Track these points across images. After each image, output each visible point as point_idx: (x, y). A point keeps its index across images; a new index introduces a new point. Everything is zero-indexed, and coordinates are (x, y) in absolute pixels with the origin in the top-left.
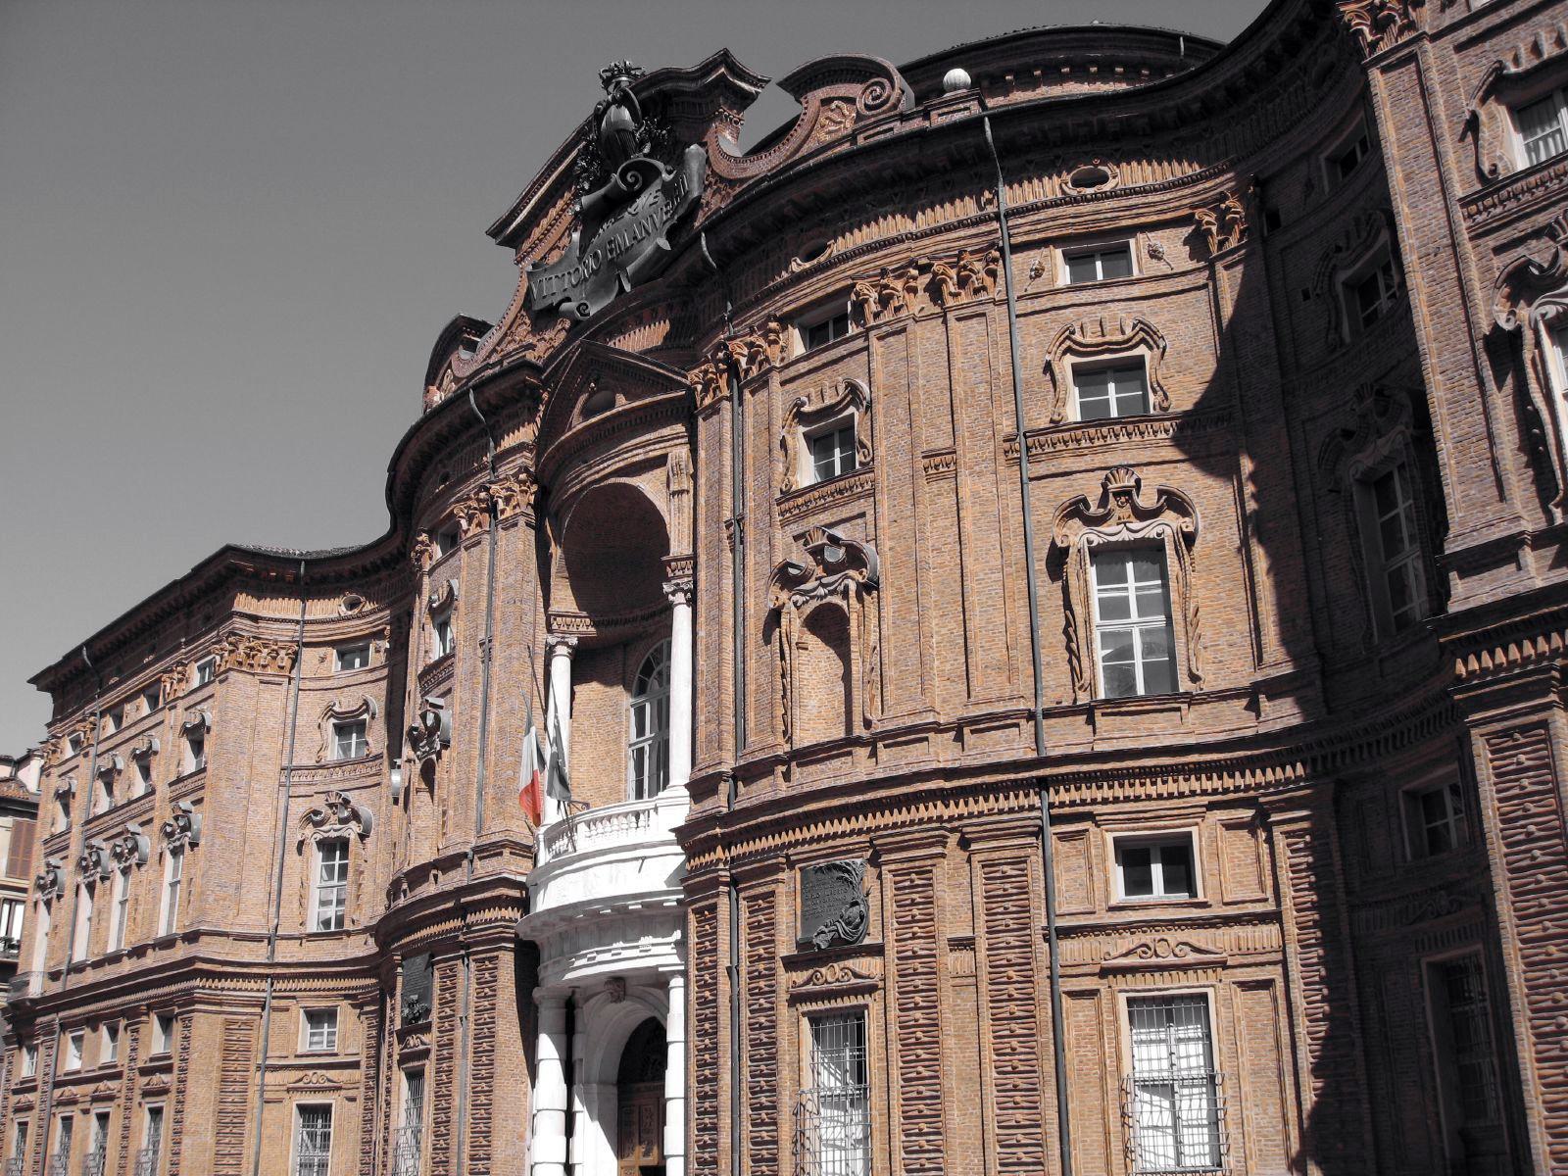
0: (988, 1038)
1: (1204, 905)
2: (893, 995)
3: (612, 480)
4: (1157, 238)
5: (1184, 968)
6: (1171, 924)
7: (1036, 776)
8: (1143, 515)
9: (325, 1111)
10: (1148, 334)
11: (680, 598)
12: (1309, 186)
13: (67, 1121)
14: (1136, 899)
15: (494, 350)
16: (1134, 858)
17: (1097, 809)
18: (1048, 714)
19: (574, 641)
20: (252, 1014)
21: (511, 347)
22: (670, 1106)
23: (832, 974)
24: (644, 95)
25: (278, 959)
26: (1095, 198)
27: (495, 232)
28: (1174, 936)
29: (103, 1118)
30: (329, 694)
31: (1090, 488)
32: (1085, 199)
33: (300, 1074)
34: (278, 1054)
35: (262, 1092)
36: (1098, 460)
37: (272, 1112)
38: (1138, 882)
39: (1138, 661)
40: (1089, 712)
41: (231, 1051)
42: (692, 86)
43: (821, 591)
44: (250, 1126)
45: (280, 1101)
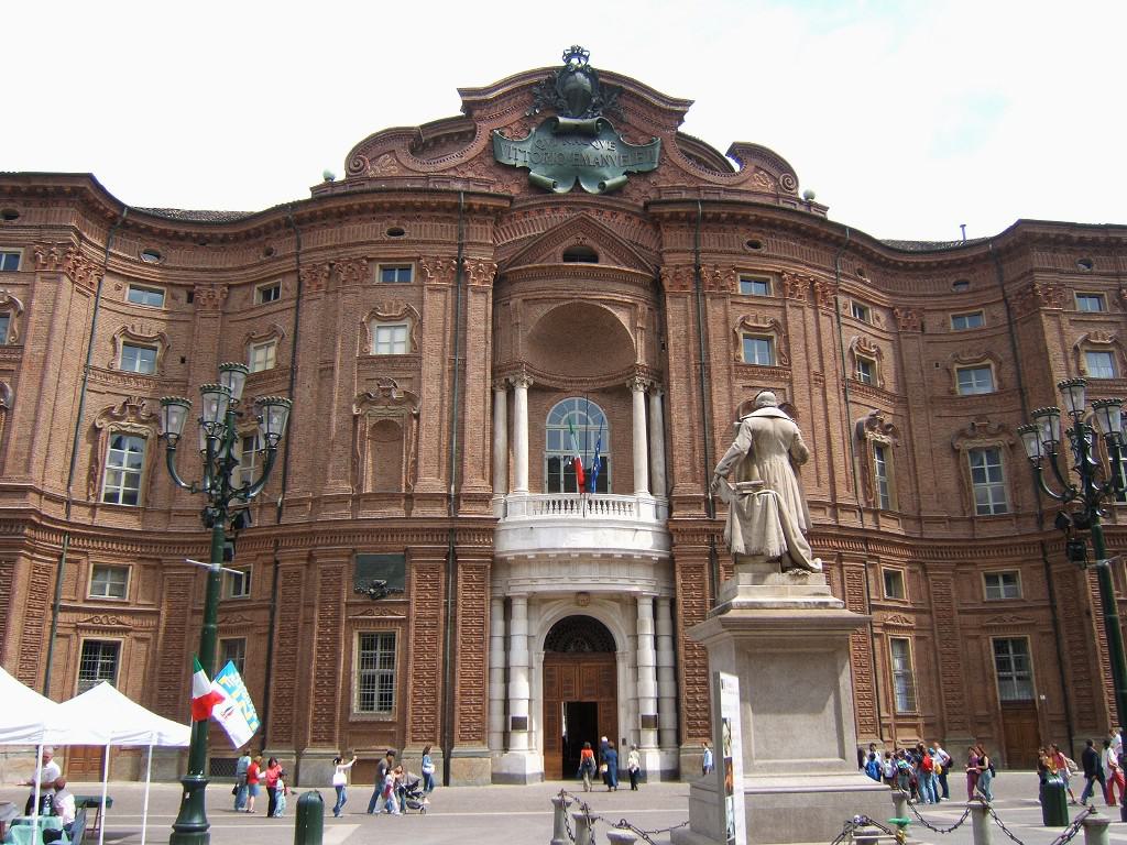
1: (906, 603)
4: (878, 312)
7: (865, 537)
9: (112, 649)
10: (879, 354)
11: (641, 388)
15: (454, 168)
20: (51, 562)
21: (470, 174)
25: (72, 520)
27: (462, 92)
33: (89, 617)
34: (66, 597)
42: (663, 105)
45: (68, 636)
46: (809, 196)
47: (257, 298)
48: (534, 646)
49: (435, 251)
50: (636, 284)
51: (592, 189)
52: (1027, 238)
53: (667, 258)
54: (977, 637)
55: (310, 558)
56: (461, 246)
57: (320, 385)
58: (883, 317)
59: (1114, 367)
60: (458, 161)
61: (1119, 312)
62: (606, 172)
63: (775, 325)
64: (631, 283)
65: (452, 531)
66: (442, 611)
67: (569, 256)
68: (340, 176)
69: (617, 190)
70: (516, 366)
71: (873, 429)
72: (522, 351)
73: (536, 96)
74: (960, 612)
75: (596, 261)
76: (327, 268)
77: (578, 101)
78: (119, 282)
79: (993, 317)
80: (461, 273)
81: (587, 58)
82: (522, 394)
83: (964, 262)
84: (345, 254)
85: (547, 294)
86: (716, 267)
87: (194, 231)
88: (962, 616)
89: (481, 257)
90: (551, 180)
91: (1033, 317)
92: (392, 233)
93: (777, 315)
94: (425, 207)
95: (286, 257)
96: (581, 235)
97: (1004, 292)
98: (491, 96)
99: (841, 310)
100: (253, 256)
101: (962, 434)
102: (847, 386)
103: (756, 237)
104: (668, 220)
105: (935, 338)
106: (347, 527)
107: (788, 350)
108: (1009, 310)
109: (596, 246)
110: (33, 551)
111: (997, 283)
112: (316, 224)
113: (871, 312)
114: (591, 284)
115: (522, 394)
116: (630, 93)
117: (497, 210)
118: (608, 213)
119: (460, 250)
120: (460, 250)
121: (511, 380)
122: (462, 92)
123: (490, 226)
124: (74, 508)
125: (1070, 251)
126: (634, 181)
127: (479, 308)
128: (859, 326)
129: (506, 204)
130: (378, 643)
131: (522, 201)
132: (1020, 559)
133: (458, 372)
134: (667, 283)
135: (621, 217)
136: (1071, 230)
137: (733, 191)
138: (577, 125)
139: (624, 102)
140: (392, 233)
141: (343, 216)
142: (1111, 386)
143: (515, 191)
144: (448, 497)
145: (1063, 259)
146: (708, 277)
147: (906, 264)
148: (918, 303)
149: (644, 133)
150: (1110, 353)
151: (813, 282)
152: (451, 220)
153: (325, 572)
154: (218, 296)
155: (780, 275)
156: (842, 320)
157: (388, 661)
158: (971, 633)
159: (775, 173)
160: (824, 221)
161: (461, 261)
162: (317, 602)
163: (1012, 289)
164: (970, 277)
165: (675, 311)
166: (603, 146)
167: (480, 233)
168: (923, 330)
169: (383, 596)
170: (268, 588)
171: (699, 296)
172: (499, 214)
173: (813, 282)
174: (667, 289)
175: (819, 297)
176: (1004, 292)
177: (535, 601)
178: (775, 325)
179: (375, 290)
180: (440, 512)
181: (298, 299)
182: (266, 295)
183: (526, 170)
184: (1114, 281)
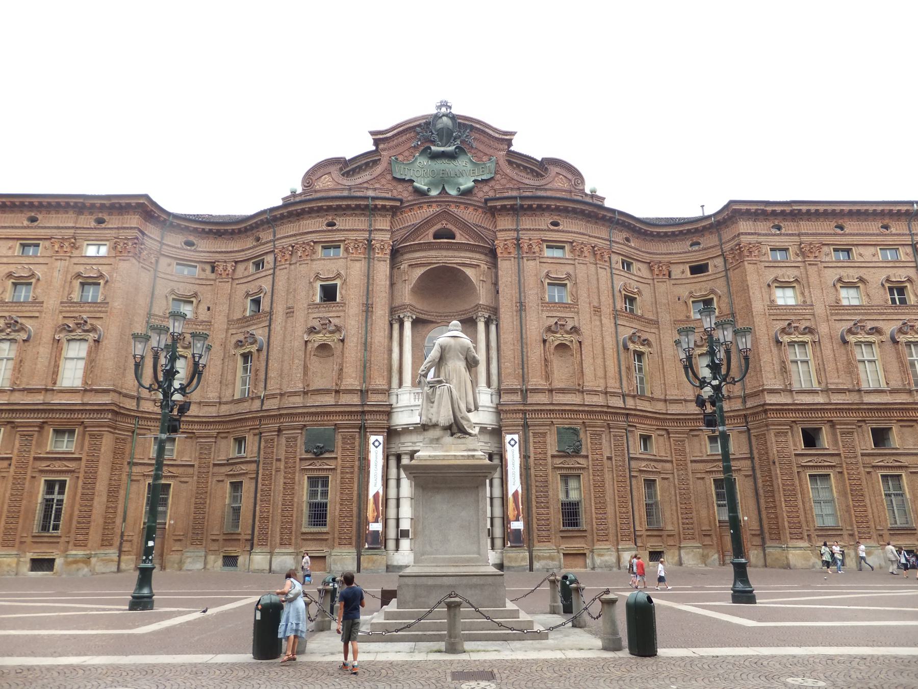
2: (591, 471)
3: (455, 266)
4: (640, 265)
10: (639, 293)
11: (483, 319)
12: (683, 272)
21: (377, 186)
23: (571, 463)
25: (141, 409)
27: (373, 133)
35: (130, 475)
37: (134, 487)
41: (117, 453)
42: (497, 135)
44: (122, 492)
46: (593, 191)
47: (251, 268)
49: (353, 236)
51: (453, 192)
52: (734, 213)
53: (499, 235)
55: (279, 430)
56: (370, 232)
57: (286, 322)
58: (644, 267)
59: (796, 297)
60: (369, 178)
61: (800, 259)
62: (461, 180)
63: (569, 276)
65: (363, 412)
66: (357, 463)
67: (436, 236)
68: (299, 190)
69: (468, 192)
70: (403, 307)
71: (633, 342)
73: (418, 133)
75: (454, 238)
76: (290, 248)
77: (446, 135)
78: (169, 260)
79: (715, 266)
81: (450, 107)
82: (408, 325)
83: (697, 230)
84: (301, 240)
85: (424, 261)
86: (530, 240)
89: (383, 238)
90: (426, 188)
91: (740, 264)
92: (329, 225)
93: (569, 269)
94: (348, 207)
95: (267, 243)
96: (444, 222)
97: (722, 248)
98: (388, 135)
99: (614, 265)
100: (250, 242)
102: (616, 314)
104: (500, 210)
105: (679, 282)
106: (300, 411)
107: (577, 292)
108: (725, 261)
109: (454, 229)
110: (115, 429)
111: (717, 243)
112: (284, 221)
113: (635, 266)
114: (450, 253)
115: (408, 325)
116: (477, 128)
117: (392, 207)
118: (462, 206)
119: (370, 234)
120: (370, 234)
121: (402, 316)
122: (373, 133)
123: (389, 218)
124: (142, 402)
125: (765, 220)
126: (479, 185)
127: (382, 269)
128: (627, 275)
129: (398, 204)
130: (318, 482)
131: (408, 201)
133: (368, 309)
134: (499, 251)
135: (471, 209)
137: (541, 190)
138: (443, 152)
139: (474, 135)
140: (329, 225)
141: (299, 215)
143: (405, 194)
144: (361, 391)
145: (763, 227)
147: (658, 233)
148: (666, 259)
149: (486, 154)
150: (794, 287)
151: (593, 247)
152: (365, 215)
153: (288, 439)
154: (229, 268)
155: (572, 243)
156: (614, 271)
157: (325, 494)
159: (570, 176)
160: (602, 208)
161: (370, 241)
162: (283, 459)
163: (727, 247)
164: (701, 240)
165: (506, 267)
166: (462, 163)
167: (383, 223)
168: (670, 276)
169: (322, 453)
170: (256, 449)
171: (520, 258)
172: (394, 210)
173: (593, 247)
174: (499, 255)
175: (598, 257)
176: (722, 248)
178: (569, 276)
179: (318, 262)
180: (355, 399)
181: (274, 268)
182: (259, 265)
183: (412, 181)
184: (796, 239)
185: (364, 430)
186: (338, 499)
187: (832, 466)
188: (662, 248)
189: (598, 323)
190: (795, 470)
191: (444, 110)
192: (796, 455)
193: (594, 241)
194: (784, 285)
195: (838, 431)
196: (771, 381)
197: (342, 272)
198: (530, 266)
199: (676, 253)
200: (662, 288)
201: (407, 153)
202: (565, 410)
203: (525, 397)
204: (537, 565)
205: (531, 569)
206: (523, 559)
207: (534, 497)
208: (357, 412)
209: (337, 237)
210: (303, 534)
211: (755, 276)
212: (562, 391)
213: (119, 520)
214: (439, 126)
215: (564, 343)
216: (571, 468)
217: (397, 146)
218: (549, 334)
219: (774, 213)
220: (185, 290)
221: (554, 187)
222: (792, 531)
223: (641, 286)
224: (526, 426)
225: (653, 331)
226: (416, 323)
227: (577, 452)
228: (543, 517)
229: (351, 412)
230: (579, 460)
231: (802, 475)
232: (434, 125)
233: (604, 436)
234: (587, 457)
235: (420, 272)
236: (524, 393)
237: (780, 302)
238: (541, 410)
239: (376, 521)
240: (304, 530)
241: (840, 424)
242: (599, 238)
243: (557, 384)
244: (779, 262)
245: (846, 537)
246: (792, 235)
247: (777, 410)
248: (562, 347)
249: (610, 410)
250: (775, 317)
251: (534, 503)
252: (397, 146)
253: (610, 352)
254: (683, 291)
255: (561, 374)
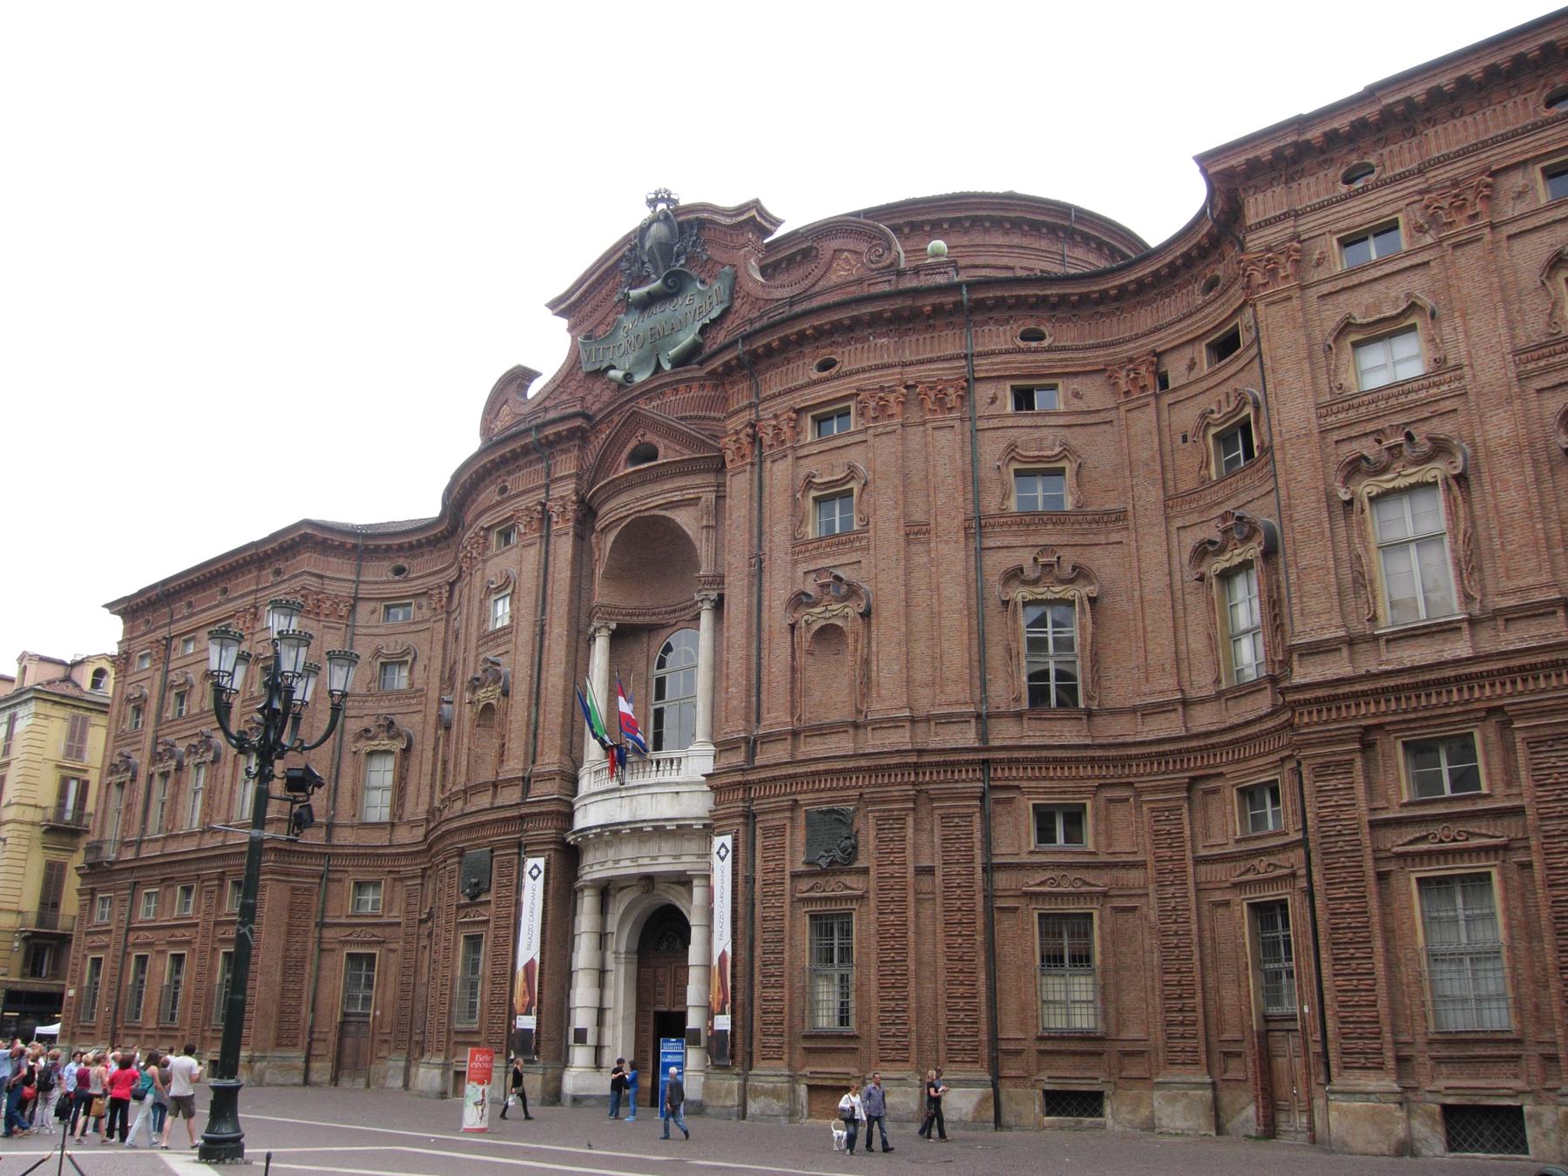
0: (940, 936)
2: (873, 903)
4: (1075, 384)
5: (1078, 896)
6: (1070, 866)
8: (1062, 582)
10: (1067, 452)
11: (707, 605)
12: (1192, 366)
13: (142, 960)
14: (1046, 846)
16: (1044, 821)
17: (1024, 784)
18: (989, 716)
19: (613, 626)
21: (564, 397)
22: (691, 971)
23: (831, 887)
24: (681, 218)
25: (335, 842)
26: (1036, 351)
27: (553, 305)
28: (1073, 875)
29: (178, 959)
30: (379, 640)
31: (1025, 558)
32: (1029, 351)
33: (349, 931)
35: (320, 941)
36: (1032, 540)
38: (1045, 834)
39: (1052, 683)
40: (1019, 715)
42: (728, 221)
43: (827, 615)
44: (309, 969)
45: (332, 950)
48: (611, 943)
50: (707, 471)
54: (1227, 904)
56: (547, 487)
64: (693, 472)
65: (521, 817)
72: (601, 594)
74: (1198, 861)
75: (655, 457)
80: (545, 518)
87: (421, 536)
88: (1203, 868)
98: (573, 299)
101: (1203, 551)
103: (825, 353)
105: (1183, 394)
114: (648, 490)
117: (572, 433)
118: (682, 387)
122: (553, 305)
129: (579, 422)
132: (1276, 757)
133: (541, 633)
134: (729, 456)
136: (1300, 132)
142: (1397, 396)
145: (1313, 188)
146: (767, 440)
158: (1218, 896)
165: (739, 485)
167: (566, 465)
168: (1164, 383)
177: (606, 891)
178: (852, 473)
180: (511, 796)
185: (522, 849)
186: (488, 973)
187: (1495, 849)
188: (1144, 319)
189: (924, 559)
190: (1369, 868)
191: (661, 206)
192: (1374, 825)
193: (912, 374)
194: (1384, 330)
195: (1519, 736)
196: (1315, 619)
197: (514, 571)
198: (780, 473)
199: (1170, 324)
200: (1145, 420)
201: (609, 319)
202: (817, 773)
203: (751, 754)
204: (753, 1107)
205: (743, 1115)
206: (729, 1093)
207: (757, 964)
208: (514, 818)
209: (507, 511)
210: (457, 1033)
211: (1280, 332)
212: (821, 730)
213: (305, 1010)
214: (647, 245)
215: (833, 624)
216: (827, 899)
217: (594, 310)
218: (803, 610)
219: (1332, 138)
220: (392, 646)
221: (831, 284)
222: (1350, 1044)
223: (1076, 439)
224: (749, 817)
225: (1114, 537)
226: (622, 637)
227: (846, 861)
228: (772, 1006)
229: (507, 819)
230: (848, 880)
231: (1397, 882)
232: (643, 246)
233: (910, 820)
234: (865, 871)
235: (611, 538)
236: (752, 745)
237: (1374, 381)
238: (774, 779)
239: (528, 1013)
240: (458, 1026)
241: (1527, 715)
242: (930, 361)
243: (813, 713)
244: (1375, 265)
245: (1534, 1067)
246: (1402, 177)
247: (1317, 700)
248: (829, 634)
249: (926, 759)
250: (1344, 434)
251: (758, 978)
252: (594, 310)
253: (955, 621)
254: (1187, 417)
255: (831, 693)
